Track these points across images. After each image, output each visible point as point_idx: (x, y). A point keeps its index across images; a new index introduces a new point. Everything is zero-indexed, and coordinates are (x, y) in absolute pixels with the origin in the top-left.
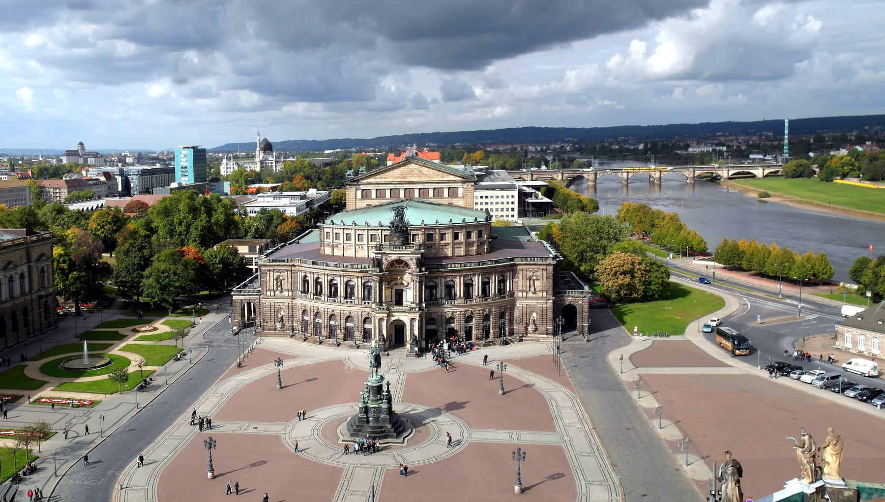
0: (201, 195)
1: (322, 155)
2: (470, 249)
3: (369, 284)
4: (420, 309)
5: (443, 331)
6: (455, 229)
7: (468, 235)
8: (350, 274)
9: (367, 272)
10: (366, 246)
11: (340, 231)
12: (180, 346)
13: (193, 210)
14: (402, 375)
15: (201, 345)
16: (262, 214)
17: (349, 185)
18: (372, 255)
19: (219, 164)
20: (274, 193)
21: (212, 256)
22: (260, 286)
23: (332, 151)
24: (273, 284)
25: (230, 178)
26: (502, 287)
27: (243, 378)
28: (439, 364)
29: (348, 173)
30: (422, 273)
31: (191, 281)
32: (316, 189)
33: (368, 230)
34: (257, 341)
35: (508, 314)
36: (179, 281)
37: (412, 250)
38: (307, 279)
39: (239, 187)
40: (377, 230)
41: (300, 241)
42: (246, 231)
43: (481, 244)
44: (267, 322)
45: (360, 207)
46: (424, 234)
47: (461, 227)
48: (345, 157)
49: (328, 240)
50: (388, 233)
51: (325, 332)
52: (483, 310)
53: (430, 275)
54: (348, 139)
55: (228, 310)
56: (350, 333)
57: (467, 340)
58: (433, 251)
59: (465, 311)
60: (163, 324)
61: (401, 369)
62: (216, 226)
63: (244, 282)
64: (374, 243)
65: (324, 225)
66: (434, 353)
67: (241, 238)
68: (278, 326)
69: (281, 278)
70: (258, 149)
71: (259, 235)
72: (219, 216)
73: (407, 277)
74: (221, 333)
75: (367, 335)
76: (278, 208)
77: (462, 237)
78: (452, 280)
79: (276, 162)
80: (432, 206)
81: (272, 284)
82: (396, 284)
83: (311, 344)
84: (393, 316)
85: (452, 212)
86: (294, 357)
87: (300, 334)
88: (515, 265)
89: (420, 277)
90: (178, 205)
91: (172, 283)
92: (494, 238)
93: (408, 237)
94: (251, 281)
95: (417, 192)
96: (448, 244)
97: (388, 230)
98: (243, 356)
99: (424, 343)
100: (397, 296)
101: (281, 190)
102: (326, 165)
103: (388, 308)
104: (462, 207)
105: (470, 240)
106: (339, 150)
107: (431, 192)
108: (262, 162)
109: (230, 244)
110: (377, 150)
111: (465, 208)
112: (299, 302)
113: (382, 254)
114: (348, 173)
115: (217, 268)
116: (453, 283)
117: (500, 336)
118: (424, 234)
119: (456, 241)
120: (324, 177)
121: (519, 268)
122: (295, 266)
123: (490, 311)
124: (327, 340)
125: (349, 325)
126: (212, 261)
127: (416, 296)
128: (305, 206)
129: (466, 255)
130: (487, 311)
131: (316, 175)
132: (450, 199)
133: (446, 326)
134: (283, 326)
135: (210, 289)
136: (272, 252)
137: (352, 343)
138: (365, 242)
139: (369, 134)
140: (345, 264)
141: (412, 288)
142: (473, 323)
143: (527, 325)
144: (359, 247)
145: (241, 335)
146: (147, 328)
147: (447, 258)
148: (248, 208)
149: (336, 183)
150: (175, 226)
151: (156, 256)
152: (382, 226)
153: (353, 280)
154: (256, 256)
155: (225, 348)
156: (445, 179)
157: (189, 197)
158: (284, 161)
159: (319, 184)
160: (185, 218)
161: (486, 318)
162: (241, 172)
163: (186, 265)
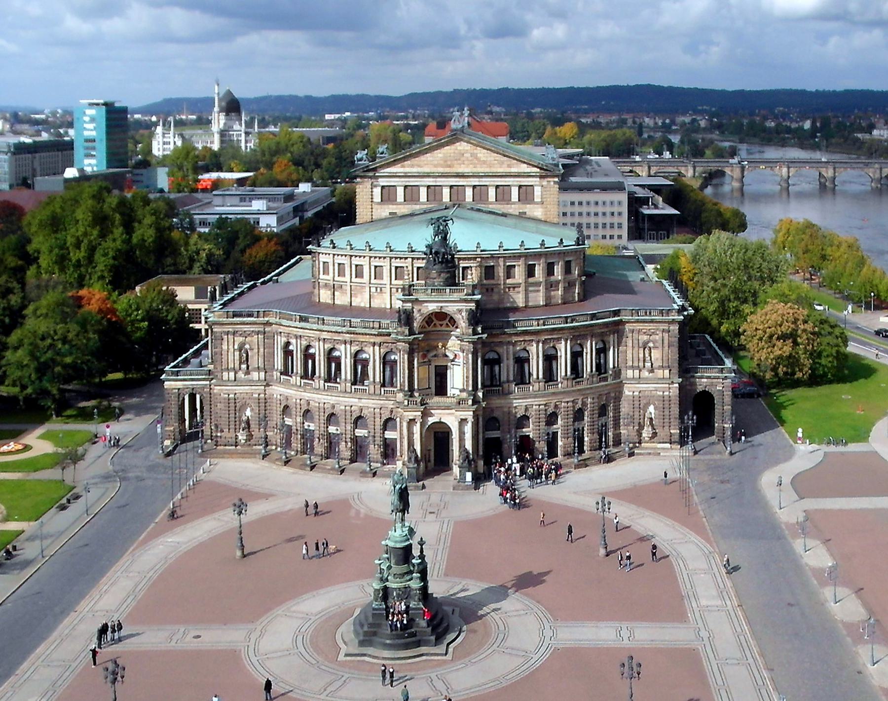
0: (116, 192)
1: (322, 122)
2: (552, 293)
3: (393, 357)
4: (475, 402)
5: (511, 442)
6: (529, 258)
7: (550, 270)
8: (361, 338)
9: (389, 335)
10: (388, 286)
11: (345, 261)
12: (69, 481)
13: (101, 221)
14: (445, 525)
15: (107, 478)
16: (218, 228)
17: (361, 177)
18: (398, 304)
19: (152, 135)
20: (242, 190)
21: (130, 307)
22: (212, 363)
23: (337, 116)
24: (232, 358)
25: (168, 162)
26: (602, 361)
27: (178, 540)
28: (506, 502)
29: (359, 156)
30: (476, 337)
31: (92, 354)
32: (310, 184)
33: (391, 258)
34: (205, 466)
35: (611, 407)
36: (71, 354)
37: (462, 296)
38: (291, 348)
39: (184, 177)
40: (406, 258)
41: (281, 278)
42: (192, 260)
43: (570, 285)
44: (222, 431)
45: (379, 217)
46: (480, 266)
47: (538, 256)
48: (360, 127)
49: (325, 277)
50: (422, 264)
51: (319, 447)
52: (573, 401)
53: (491, 340)
54: (363, 96)
55: (156, 408)
56: (361, 447)
57: (549, 458)
58: (495, 297)
59: (545, 405)
60: (42, 437)
61: (444, 514)
62: (140, 250)
63: (184, 356)
64: (400, 282)
65: (319, 250)
66: (498, 482)
67: (181, 273)
68: (242, 437)
69: (247, 346)
70: (216, 109)
71: (213, 267)
72: (145, 232)
73: (453, 344)
74: (143, 453)
75: (388, 451)
76: (246, 216)
77: (539, 272)
78: (525, 349)
79: (247, 134)
80: (493, 216)
81: (231, 358)
82: (435, 356)
83: (297, 470)
84: (432, 415)
85: (525, 229)
86: (267, 496)
87: (277, 451)
88: (621, 323)
89: (473, 343)
90: (74, 212)
91: (58, 358)
92: (589, 275)
93: (455, 271)
94: (197, 353)
95: (469, 192)
96: (518, 285)
97: (423, 259)
98: (179, 496)
99: (481, 463)
100: (438, 379)
101: (254, 185)
102: (329, 140)
103: (422, 400)
104: (540, 220)
105: (552, 278)
106: (348, 114)
107: (492, 192)
108: (223, 133)
109: (162, 283)
110: (410, 116)
111: (546, 222)
112: (277, 391)
113: (412, 301)
114: (359, 156)
115: (139, 329)
116: (526, 355)
117: (600, 448)
118: (480, 266)
119: (531, 280)
120: (325, 163)
121: (628, 327)
122: (271, 324)
123: (584, 404)
124: (324, 461)
125: (360, 432)
126: (130, 315)
127: (467, 377)
128: (292, 215)
129: (546, 305)
130: (580, 402)
131: (312, 158)
132: (521, 206)
133: (516, 432)
134: (250, 437)
135: (126, 371)
136: (233, 299)
137: (365, 466)
138: (386, 280)
139: (397, 89)
140: (353, 320)
141: (462, 364)
142: (559, 426)
143: (641, 427)
144: (377, 290)
145: (176, 457)
146: (12, 446)
147: (516, 309)
148: (195, 217)
149: (344, 174)
150: (68, 248)
151: (31, 308)
152: (413, 251)
153: (366, 349)
154: (206, 306)
155: (149, 482)
156: (514, 170)
157: (94, 197)
158: (259, 133)
159: (316, 175)
160: (85, 234)
161: (578, 415)
162: (187, 150)
163: (84, 324)
